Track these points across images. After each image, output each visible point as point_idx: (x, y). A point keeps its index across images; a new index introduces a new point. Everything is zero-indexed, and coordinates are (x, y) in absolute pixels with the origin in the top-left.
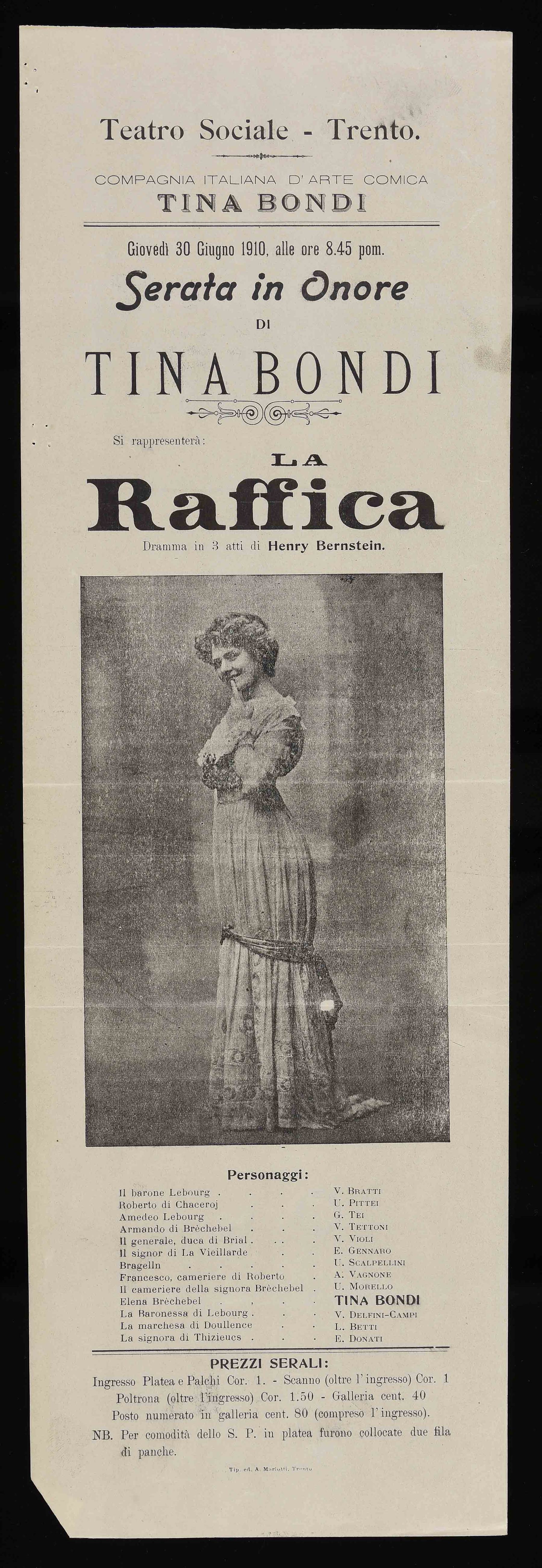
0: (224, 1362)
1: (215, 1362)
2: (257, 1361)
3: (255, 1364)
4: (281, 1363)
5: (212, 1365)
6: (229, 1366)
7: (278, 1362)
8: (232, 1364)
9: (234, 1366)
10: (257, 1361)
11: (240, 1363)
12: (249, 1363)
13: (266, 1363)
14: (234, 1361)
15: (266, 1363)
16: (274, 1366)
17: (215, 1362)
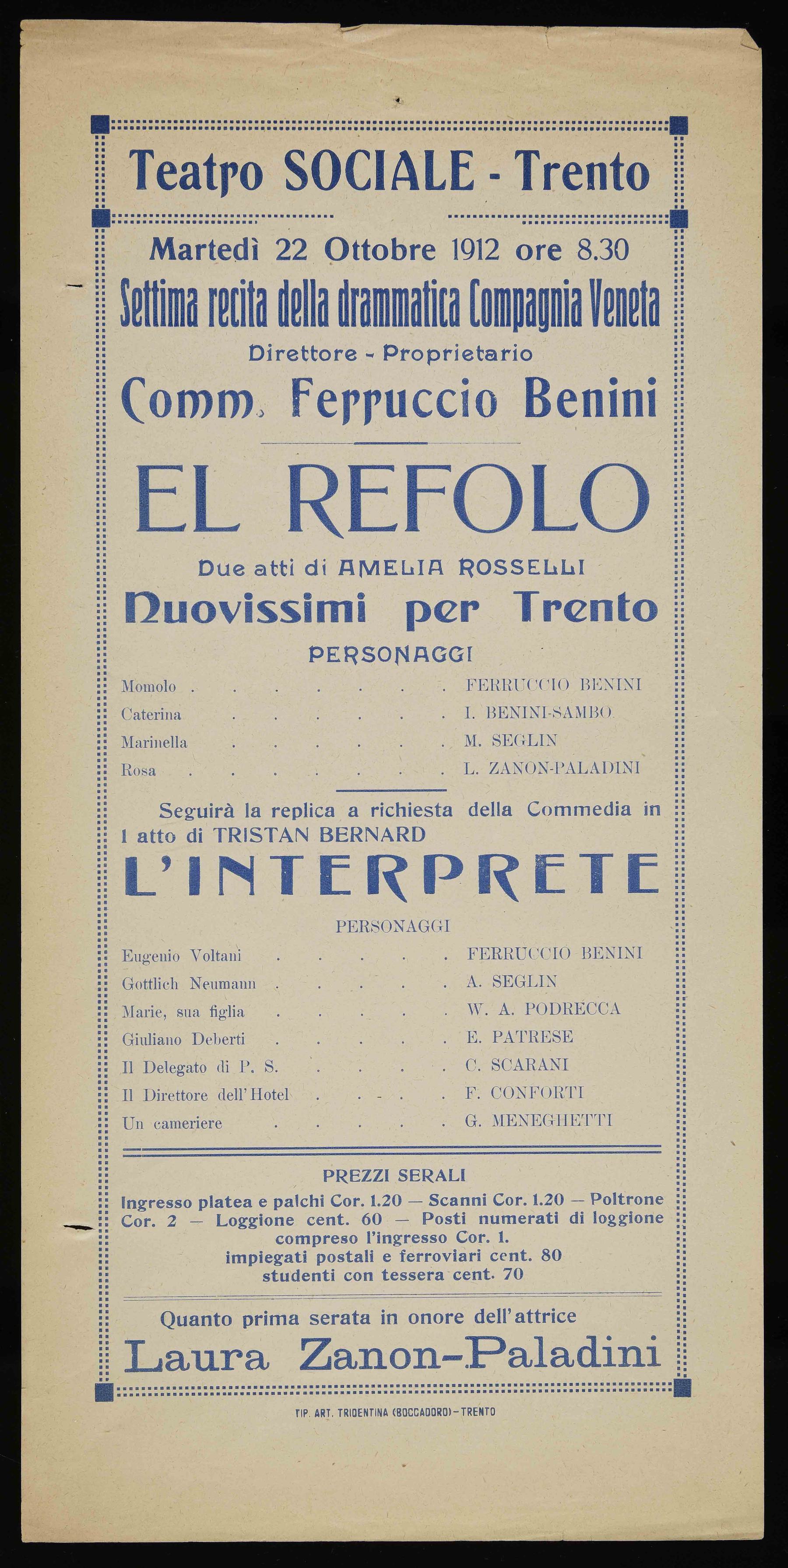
0: (342, 1174)
1: (329, 1173)
2: (383, 1173)
3: (382, 1175)
4: (412, 1175)
5: (326, 1177)
6: (347, 1178)
7: (408, 1174)
8: (352, 1176)
9: (355, 1178)
10: (383, 1173)
11: (362, 1175)
12: (372, 1175)
13: (394, 1175)
14: (355, 1173)
15: (394, 1175)
16: (403, 1178)
17: (329, 1173)
